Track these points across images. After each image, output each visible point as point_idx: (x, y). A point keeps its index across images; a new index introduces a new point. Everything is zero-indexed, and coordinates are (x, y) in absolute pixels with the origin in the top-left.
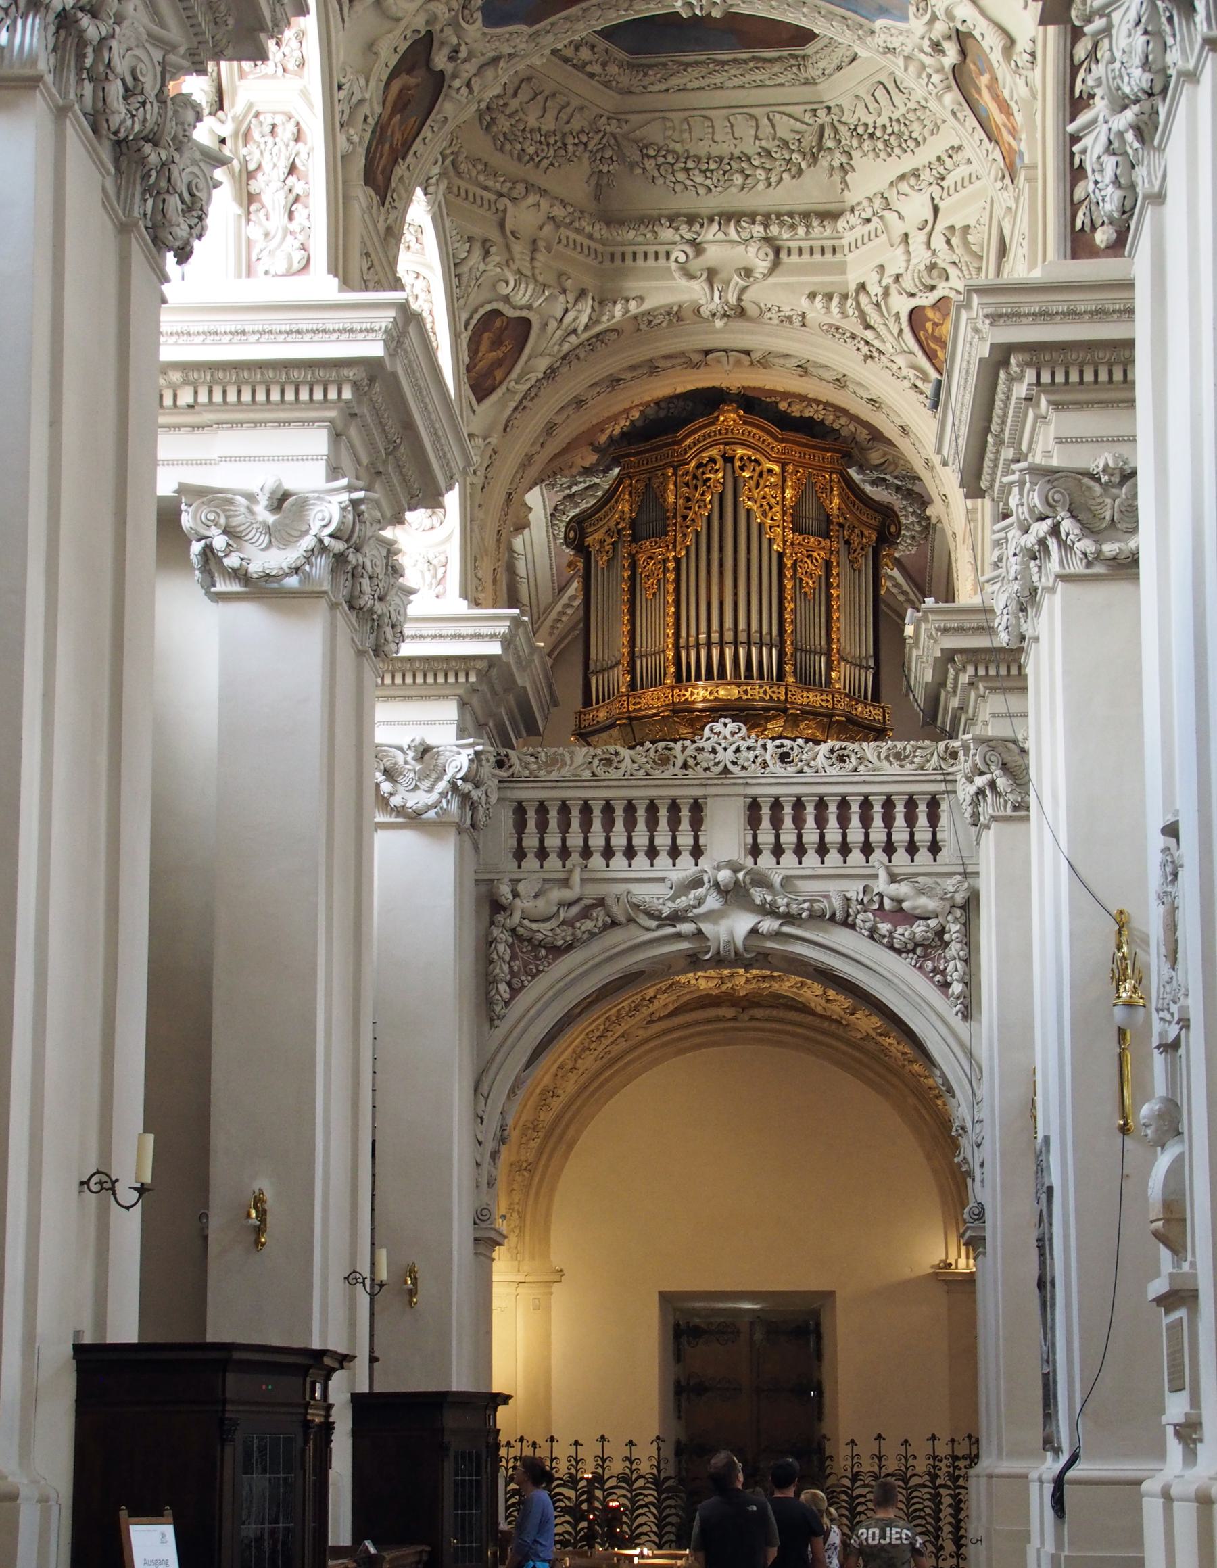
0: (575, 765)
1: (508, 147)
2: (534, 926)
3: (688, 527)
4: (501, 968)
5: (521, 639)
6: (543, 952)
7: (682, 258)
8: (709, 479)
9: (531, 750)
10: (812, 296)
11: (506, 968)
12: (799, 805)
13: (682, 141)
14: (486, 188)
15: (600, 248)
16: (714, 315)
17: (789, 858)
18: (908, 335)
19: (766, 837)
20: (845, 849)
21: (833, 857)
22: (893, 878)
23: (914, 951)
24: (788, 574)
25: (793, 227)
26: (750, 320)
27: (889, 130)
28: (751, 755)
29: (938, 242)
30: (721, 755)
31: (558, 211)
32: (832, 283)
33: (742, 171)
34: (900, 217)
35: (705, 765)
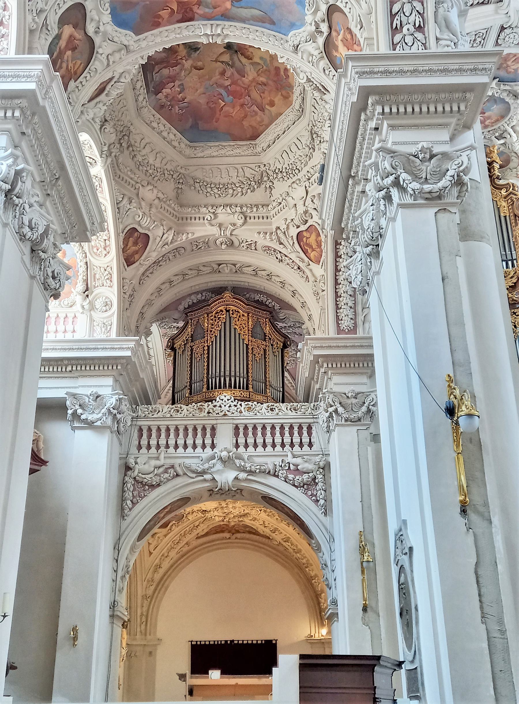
1: (141, 168)
2: (143, 476)
3: (212, 334)
4: (128, 494)
6: (147, 487)
7: (209, 219)
8: (220, 317)
10: (259, 233)
11: (131, 494)
12: (255, 428)
13: (210, 177)
17: (251, 449)
18: (296, 245)
19: (241, 440)
21: (269, 448)
22: (294, 456)
23: (303, 487)
26: (236, 248)
30: (223, 408)
32: (266, 229)
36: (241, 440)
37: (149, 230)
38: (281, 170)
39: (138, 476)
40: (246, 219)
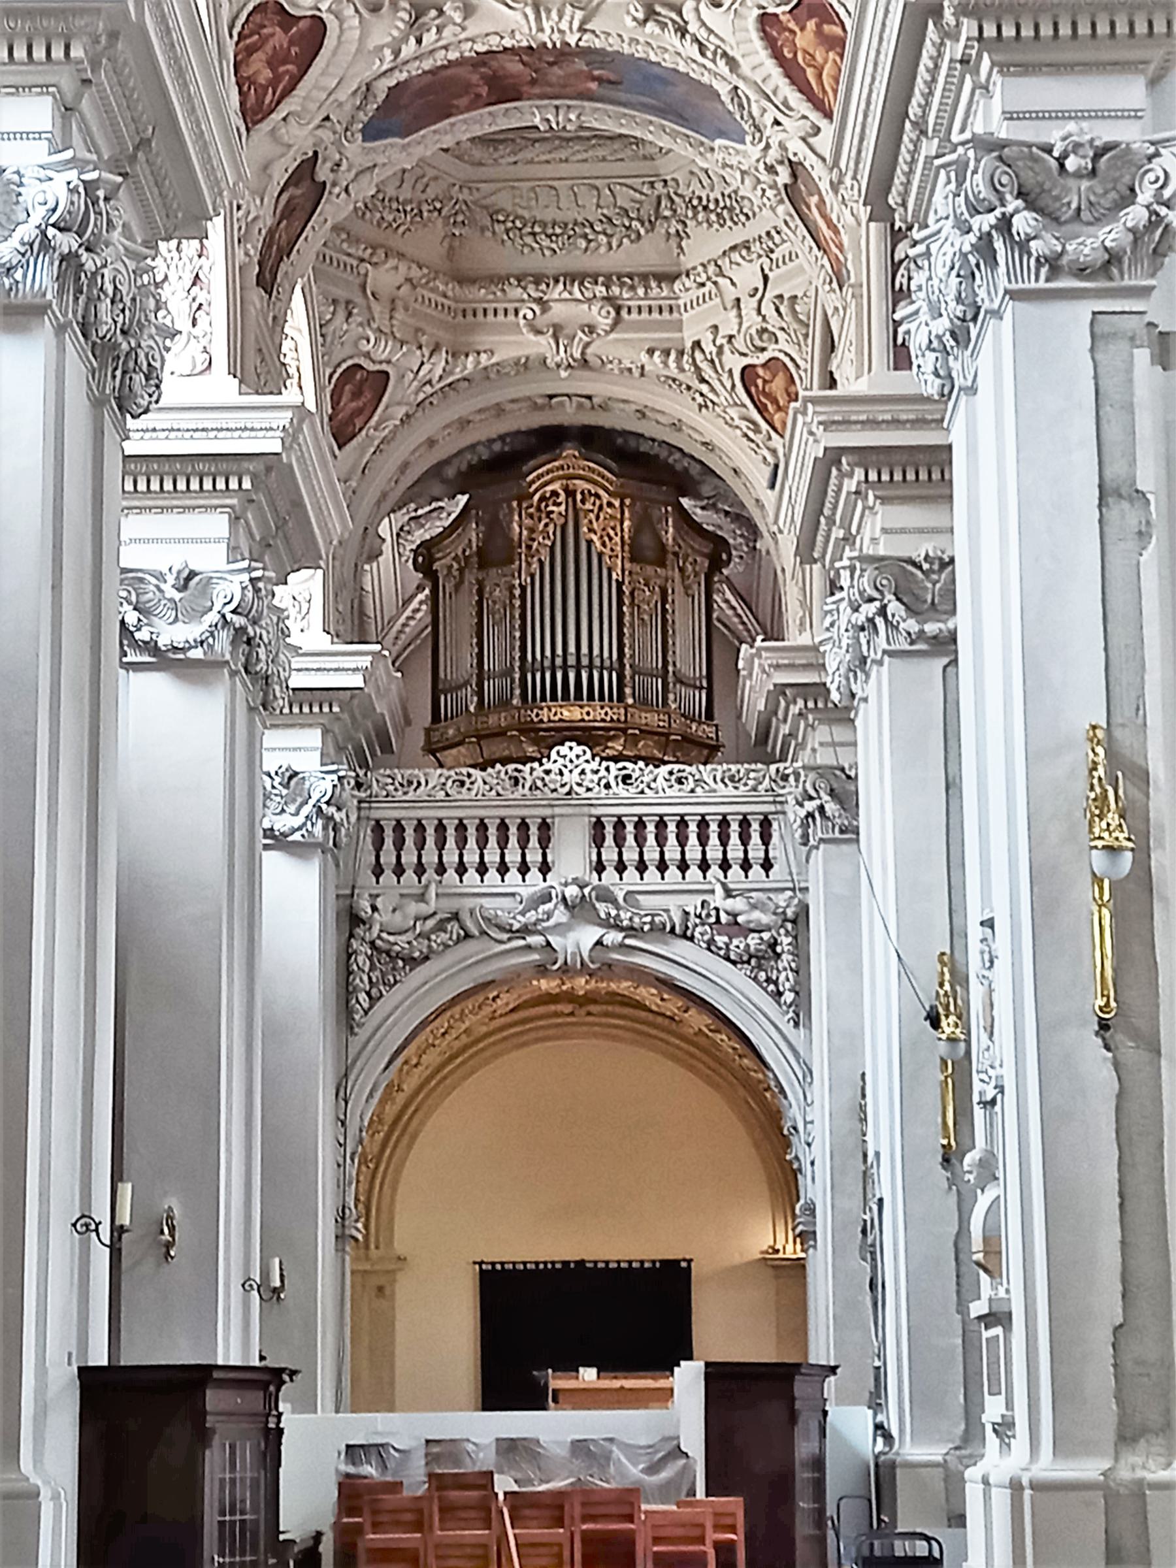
0: (430, 785)
2: (392, 939)
5: (381, 671)
6: (401, 963)
7: (530, 315)
9: (388, 772)
10: (651, 352)
11: (365, 978)
12: (640, 824)
13: (528, 208)
14: (349, 255)
15: (453, 305)
16: (558, 366)
17: (631, 874)
20: (683, 867)
21: (673, 872)
23: (748, 962)
25: (632, 288)
27: (722, 204)
28: (596, 778)
29: (768, 309)
30: (566, 778)
31: (415, 273)
32: (668, 339)
33: (585, 236)
34: (733, 284)
35: (552, 786)
37: (389, 362)
38: (704, 202)
39: (379, 937)
40: (618, 313)
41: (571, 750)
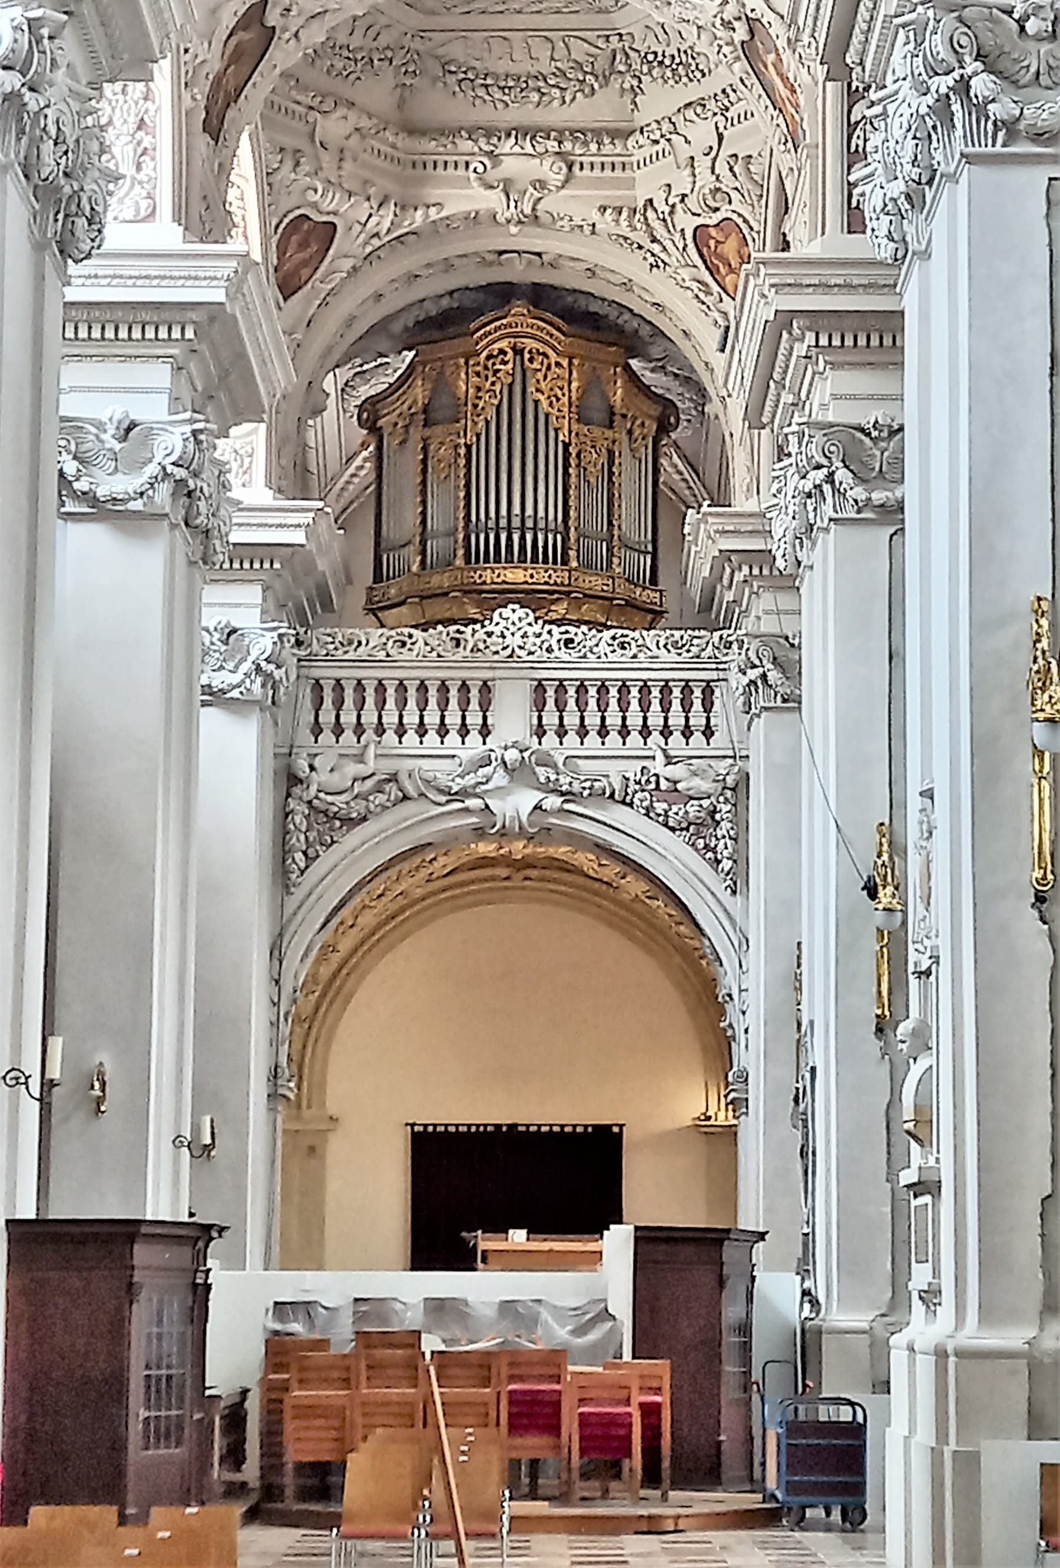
6: (338, 823)
7: (480, 169)
9: (328, 631)
10: (603, 209)
11: (302, 837)
14: (299, 103)
15: (402, 156)
16: (509, 221)
17: (572, 739)
21: (614, 738)
22: (669, 760)
24: (573, 462)
25: (586, 144)
27: (677, 60)
28: (538, 641)
29: (722, 168)
30: (508, 641)
31: (365, 123)
34: (687, 141)
35: (493, 648)
36: (550, 718)
37: (335, 213)
38: (660, 58)
39: (317, 797)
40: (570, 168)
41: (513, 613)
